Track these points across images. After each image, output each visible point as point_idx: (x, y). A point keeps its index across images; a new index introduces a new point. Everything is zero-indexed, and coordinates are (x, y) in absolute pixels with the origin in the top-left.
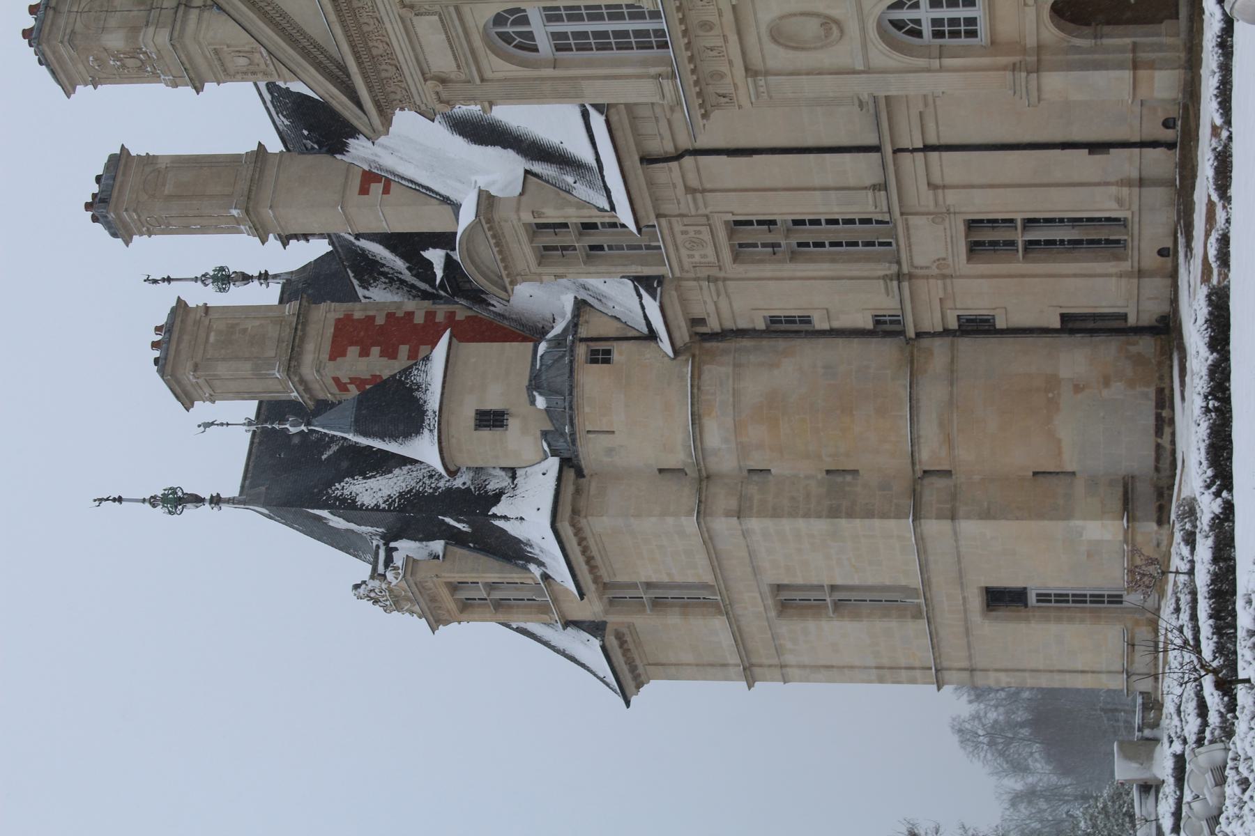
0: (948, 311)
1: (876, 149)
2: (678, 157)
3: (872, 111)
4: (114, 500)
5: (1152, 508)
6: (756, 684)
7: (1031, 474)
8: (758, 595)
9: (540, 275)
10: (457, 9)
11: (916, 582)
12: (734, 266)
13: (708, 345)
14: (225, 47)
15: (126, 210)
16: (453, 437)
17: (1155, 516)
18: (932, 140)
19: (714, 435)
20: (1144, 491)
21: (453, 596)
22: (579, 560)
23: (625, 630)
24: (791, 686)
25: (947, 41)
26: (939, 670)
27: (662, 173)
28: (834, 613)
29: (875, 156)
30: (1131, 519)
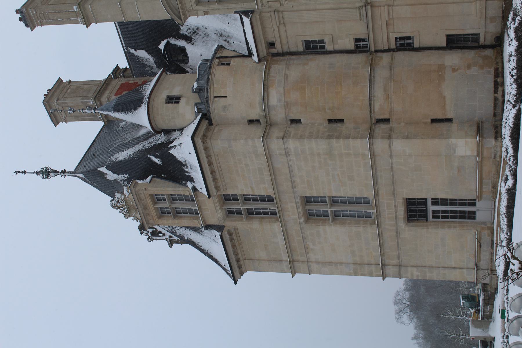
0: (391, 34)
4: (22, 172)
5: (492, 132)
6: (296, 274)
7: (430, 121)
8: (295, 205)
9: (197, 10)
13: (275, 58)
15: (31, 9)
16: (155, 107)
17: (493, 136)
19: (274, 99)
20: (488, 127)
21: (154, 206)
22: (203, 155)
23: (233, 230)
26: (385, 265)
28: (332, 222)
30: (481, 136)
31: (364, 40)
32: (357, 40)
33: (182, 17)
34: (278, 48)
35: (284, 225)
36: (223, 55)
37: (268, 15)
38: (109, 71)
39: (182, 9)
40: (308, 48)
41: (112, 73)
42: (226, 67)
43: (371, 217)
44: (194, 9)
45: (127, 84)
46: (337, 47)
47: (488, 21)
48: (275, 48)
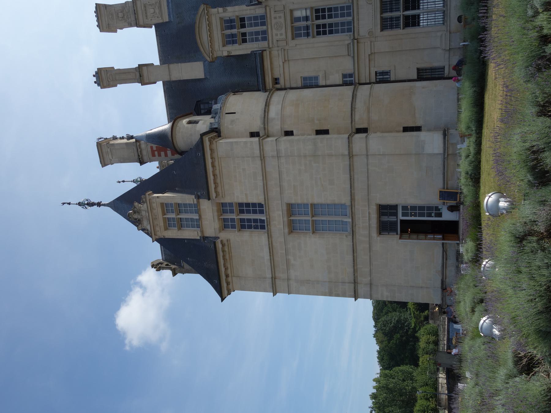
6: (278, 294)
8: (281, 213)
11: (348, 203)
16: (178, 126)
21: (163, 216)
23: (225, 242)
24: (290, 295)
28: (312, 234)
35: (270, 237)
43: (347, 216)
44: (221, 50)
46: (328, 83)
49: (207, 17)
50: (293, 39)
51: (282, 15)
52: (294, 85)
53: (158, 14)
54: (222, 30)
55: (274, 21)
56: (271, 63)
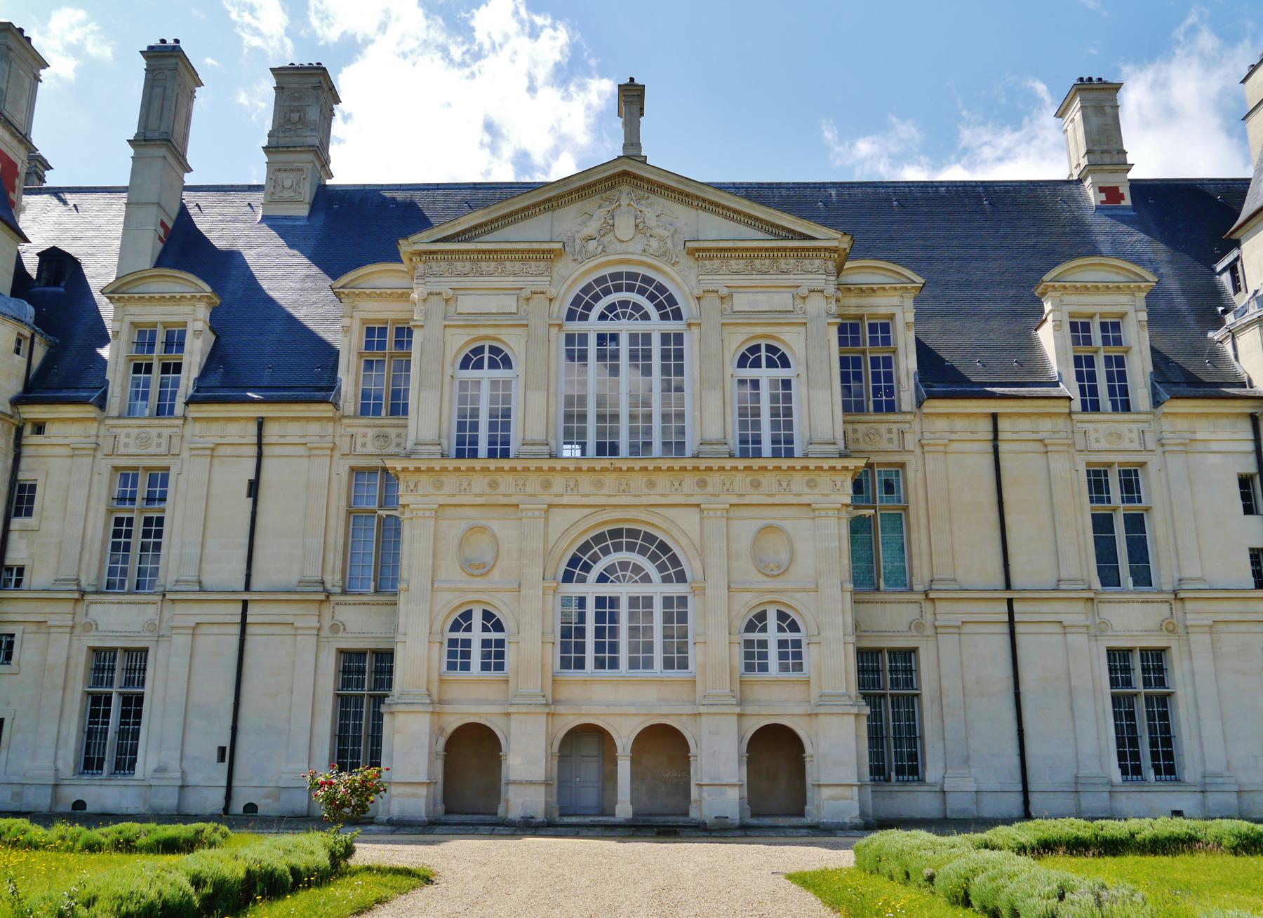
1: (247, 588)
2: (260, 444)
3: (298, 589)
9: (122, 321)
10: (527, 325)
12: (348, 466)
13: (13, 430)
14: (304, 176)
18: (250, 630)
25: (446, 648)
27: (253, 428)
29: (241, 587)
31: (18, 582)
32: (21, 570)
33: (116, 296)
34: (30, 438)
36: (36, 347)
37: (94, 432)
38: (44, 150)
39: (130, 298)
40: (22, 487)
41: (40, 156)
42: (13, 345)
44: (126, 317)
45: (16, 174)
47: (16, 789)
48: (33, 433)
49: (188, 296)
50: (116, 468)
51: (163, 450)
52: (24, 463)
53: (281, 195)
54: (165, 325)
55: (154, 432)
56: (73, 420)
